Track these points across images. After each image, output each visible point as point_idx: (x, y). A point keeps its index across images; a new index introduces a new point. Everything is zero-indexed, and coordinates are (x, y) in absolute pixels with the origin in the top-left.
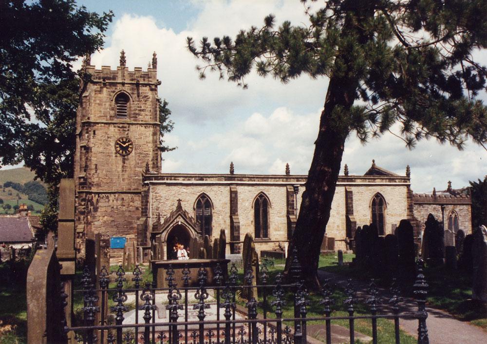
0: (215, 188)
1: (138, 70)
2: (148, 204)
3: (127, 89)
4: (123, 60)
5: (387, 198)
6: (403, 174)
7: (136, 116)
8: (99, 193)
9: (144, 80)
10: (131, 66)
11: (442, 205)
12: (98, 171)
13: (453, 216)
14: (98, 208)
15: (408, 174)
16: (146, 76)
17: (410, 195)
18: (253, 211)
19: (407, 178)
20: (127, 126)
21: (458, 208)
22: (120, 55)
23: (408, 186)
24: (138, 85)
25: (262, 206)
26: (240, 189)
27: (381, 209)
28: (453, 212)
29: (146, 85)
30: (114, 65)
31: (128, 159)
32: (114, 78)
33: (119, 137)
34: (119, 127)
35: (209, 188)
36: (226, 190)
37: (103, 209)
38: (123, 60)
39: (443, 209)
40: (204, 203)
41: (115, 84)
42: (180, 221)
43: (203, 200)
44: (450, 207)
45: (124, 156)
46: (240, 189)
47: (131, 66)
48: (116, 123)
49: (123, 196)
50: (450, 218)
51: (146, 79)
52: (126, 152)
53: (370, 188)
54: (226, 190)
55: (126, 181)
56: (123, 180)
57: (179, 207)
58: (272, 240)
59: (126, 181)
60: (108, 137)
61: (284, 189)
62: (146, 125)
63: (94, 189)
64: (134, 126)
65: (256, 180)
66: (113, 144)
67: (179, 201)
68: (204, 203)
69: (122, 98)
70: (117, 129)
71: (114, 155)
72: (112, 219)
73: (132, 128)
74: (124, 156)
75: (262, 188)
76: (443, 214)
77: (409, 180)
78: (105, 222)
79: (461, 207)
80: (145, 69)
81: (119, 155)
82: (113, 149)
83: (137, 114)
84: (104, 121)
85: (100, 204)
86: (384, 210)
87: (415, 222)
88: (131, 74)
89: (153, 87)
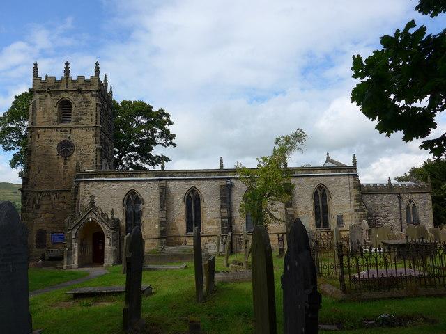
0: (144, 184)
1: (81, 78)
2: (77, 202)
3: (69, 97)
4: (67, 70)
5: (331, 189)
6: (350, 164)
7: (77, 120)
8: (41, 192)
9: (86, 87)
10: (74, 75)
11: (399, 194)
12: (41, 172)
13: (411, 205)
14: (39, 206)
15: (355, 163)
16: (87, 83)
17: (358, 185)
18: (184, 207)
19: (354, 168)
20: (69, 129)
21: (416, 197)
22: (65, 66)
23: (356, 175)
24: (79, 91)
25: (193, 202)
26: (170, 184)
27: (324, 200)
28: (410, 201)
29: (88, 91)
30: (59, 74)
31: (69, 160)
32: (58, 87)
33: (62, 140)
34: (61, 131)
35: (138, 185)
36: (155, 186)
37: (45, 207)
38: (67, 70)
39: (400, 198)
40: (133, 200)
41: (58, 92)
42: (92, 217)
43: (133, 196)
44: (408, 197)
45: (65, 157)
46: (170, 184)
47: (74, 75)
48: (58, 128)
49: (64, 194)
50: (408, 207)
51: (88, 87)
52: (67, 153)
53: (312, 179)
54: (155, 186)
55: (67, 181)
56: (65, 179)
57: (92, 204)
58: (205, 235)
59: (67, 181)
60: (51, 141)
61: (217, 183)
62: (87, 128)
63: (37, 189)
64: (75, 130)
65: (204, 174)
66: (55, 147)
67: (93, 196)
68: (133, 200)
69: (65, 105)
70: (59, 133)
71: (56, 157)
72: (53, 215)
73: (74, 131)
74: (65, 157)
75: (193, 182)
76: (400, 203)
77: (356, 170)
78: (46, 218)
79: (421, 196)
80: (88, 78)
81: (60, 157)
82: (56, 152)
83: (79, 118)
84: (47, 126)
85: (43, 202)
86: (329, 200)
87: (362, 213)
88: (74, 82)
89: (94, 93)
